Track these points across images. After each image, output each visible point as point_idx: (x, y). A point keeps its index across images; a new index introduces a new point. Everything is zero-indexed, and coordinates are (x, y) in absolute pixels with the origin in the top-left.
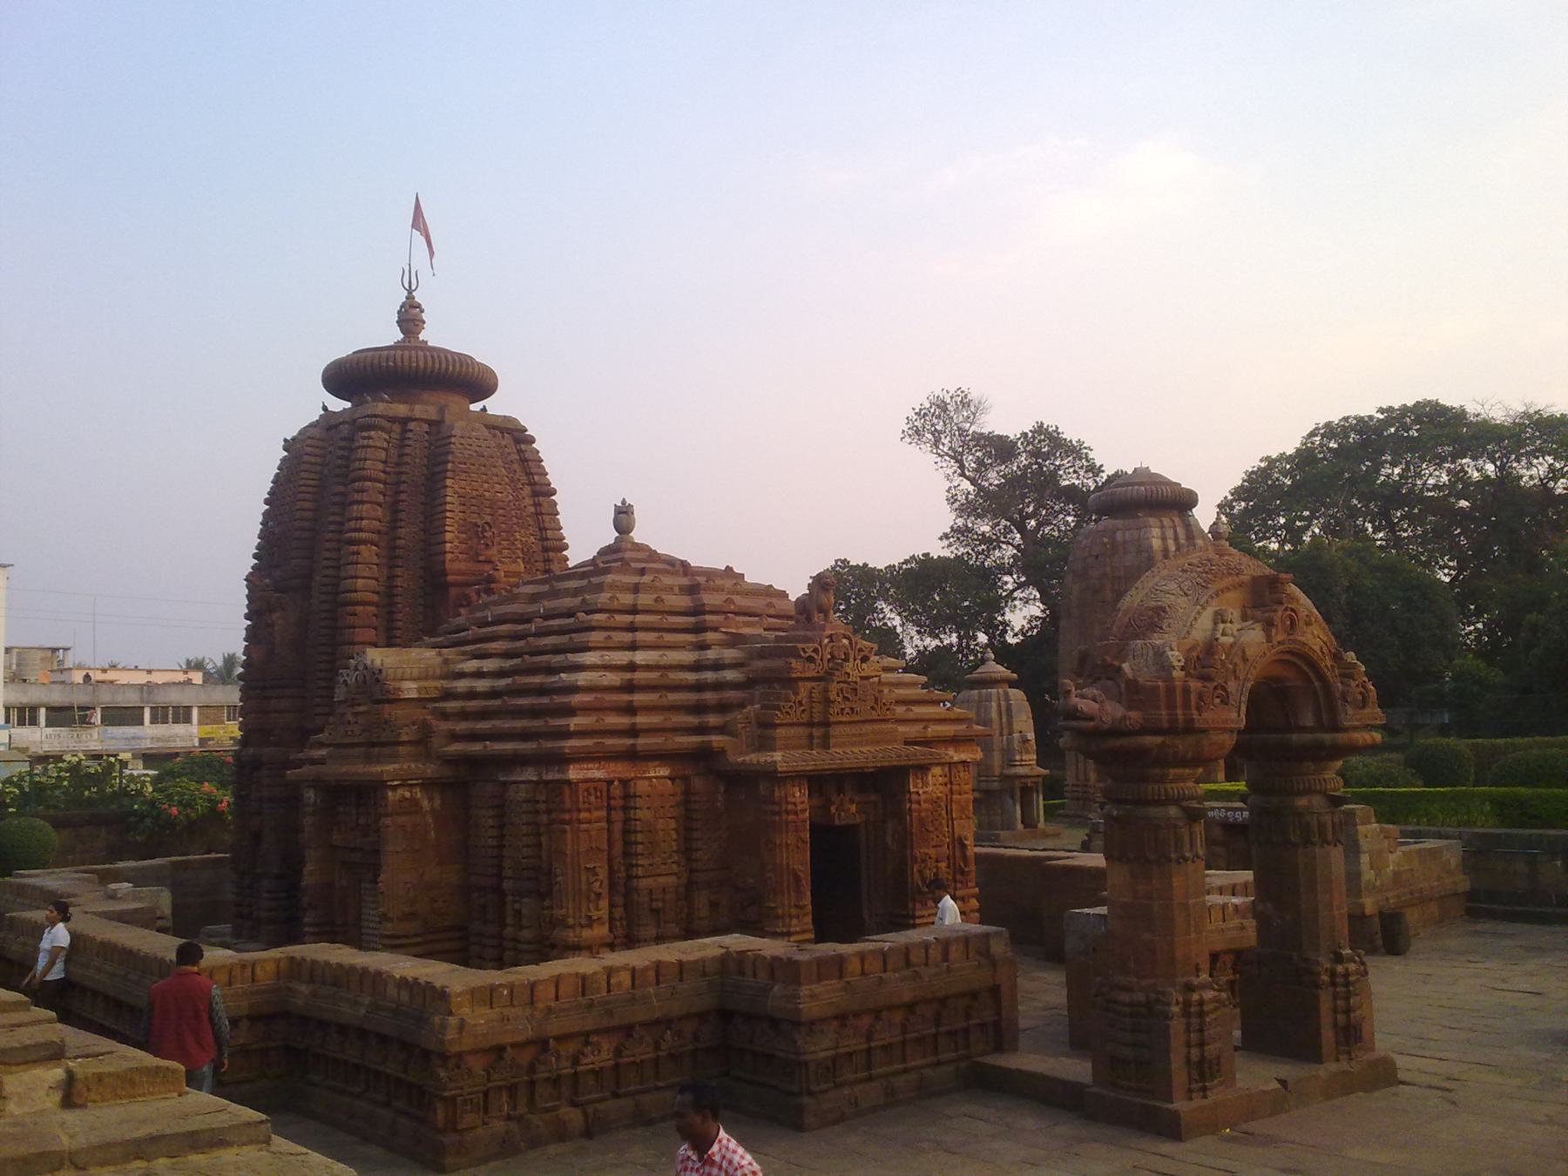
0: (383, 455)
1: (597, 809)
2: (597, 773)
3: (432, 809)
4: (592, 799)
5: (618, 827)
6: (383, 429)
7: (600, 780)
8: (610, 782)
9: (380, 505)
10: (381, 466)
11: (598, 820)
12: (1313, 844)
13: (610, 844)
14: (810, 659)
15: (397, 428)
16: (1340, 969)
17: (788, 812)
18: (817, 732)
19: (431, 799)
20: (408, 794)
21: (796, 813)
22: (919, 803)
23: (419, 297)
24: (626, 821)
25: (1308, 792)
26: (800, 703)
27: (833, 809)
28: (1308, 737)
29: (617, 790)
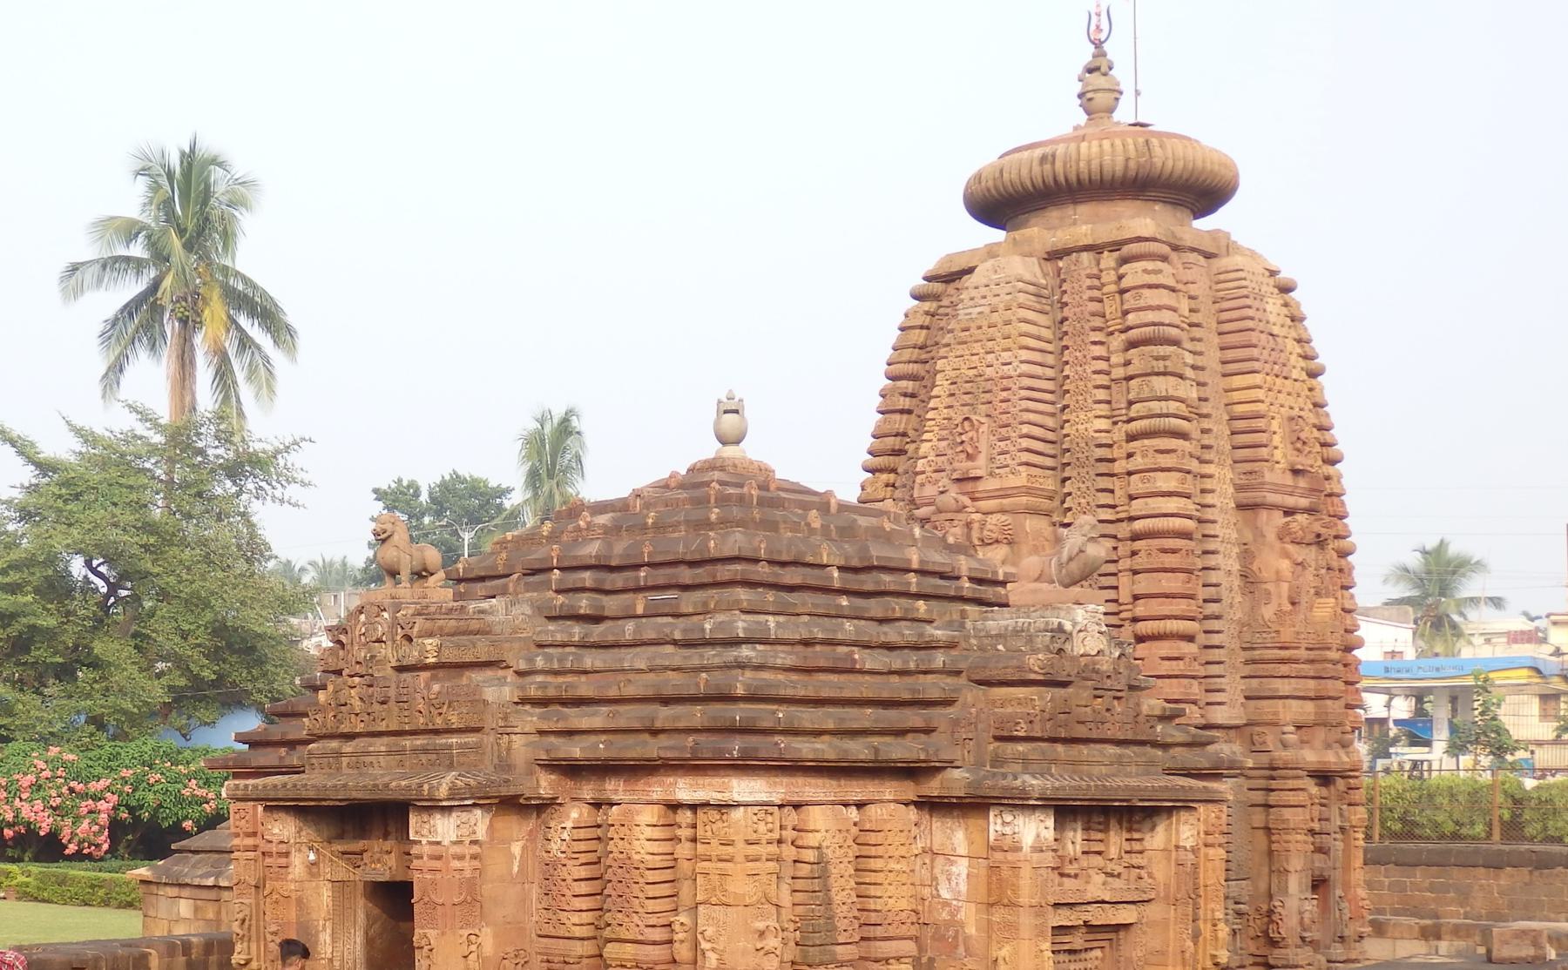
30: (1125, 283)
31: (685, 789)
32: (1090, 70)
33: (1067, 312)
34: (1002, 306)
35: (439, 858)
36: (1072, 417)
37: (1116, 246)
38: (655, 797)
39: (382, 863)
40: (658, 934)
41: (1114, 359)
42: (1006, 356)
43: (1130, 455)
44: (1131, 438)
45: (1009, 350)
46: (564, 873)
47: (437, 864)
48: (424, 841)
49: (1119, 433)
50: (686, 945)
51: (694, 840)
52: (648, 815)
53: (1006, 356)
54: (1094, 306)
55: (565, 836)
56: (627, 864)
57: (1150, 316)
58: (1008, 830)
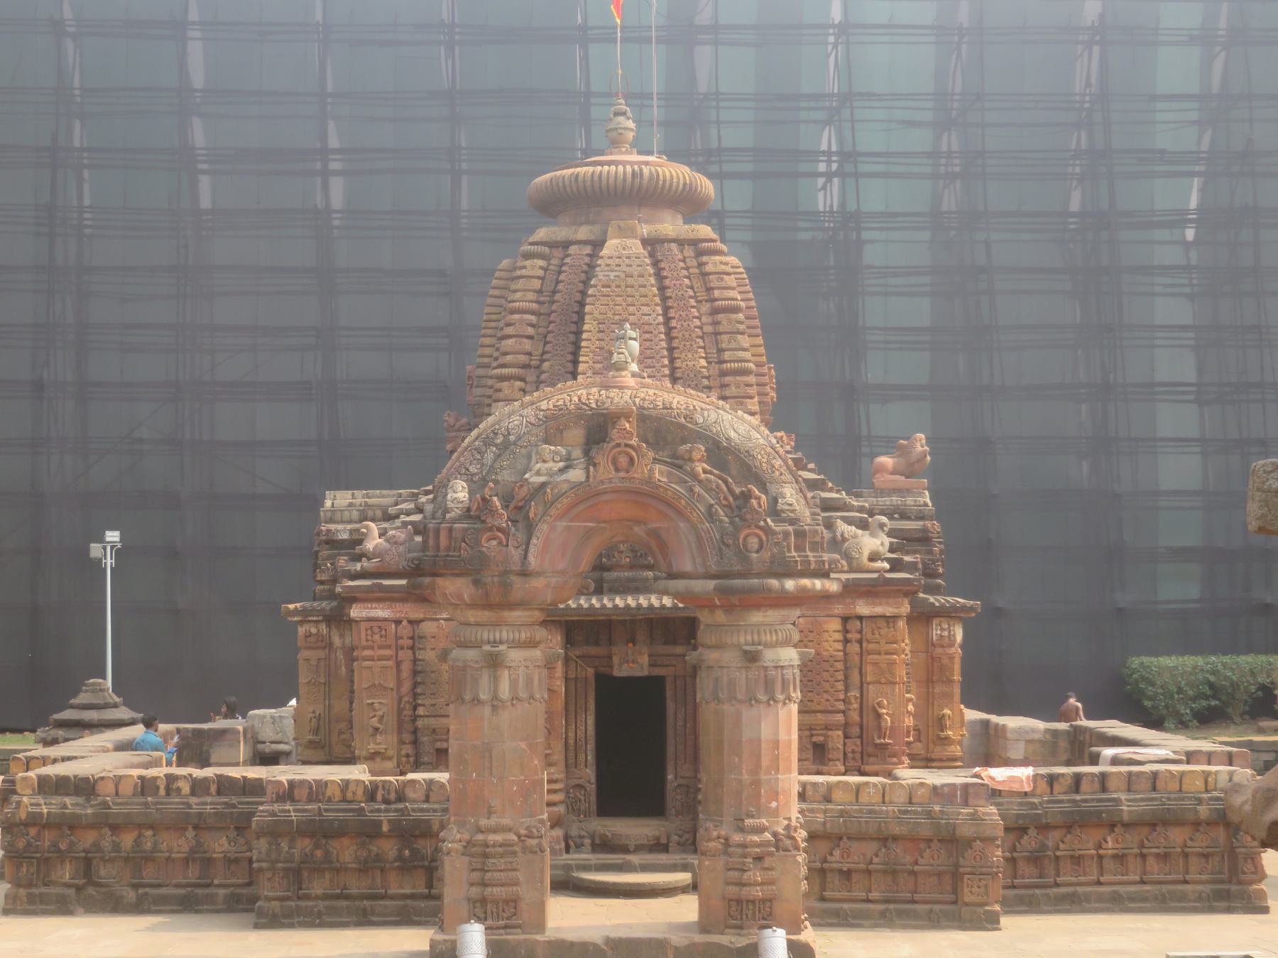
0: (537, 284)
1: (380, 647)
2: (381, 612)
3: (344, 646)
4: (377, 637)
5: (406, 668)
7: (385, 620)
8: (398, 622)
9: (530, 337)
10: (531, 296)
11: (387, 658)
13: (399, 683)
15: (558, 253)
16: (737, 838)
19: (342, 636)
20: (314, 630)
24: (415, 661)
25: (718, 647)
27: (616, 660)
29: (405, 630)
31: (863, 609)
33: (667, 282)
34: (636, 273)
36: (683, 356)
37: (694, 242)
38: (836, 611)
39: (633, 663)
40: (841, 706)
41: (704, 319)
42: (645, 309)
43: (723, 386)
44: (723, 374)
45: (647, 305)
49: (715, 369)
50: (857, 712)
51: (860, 642)
52: (835, 625)
53: (645, 309)
54: (687, 281)
57: (731, 294)
58: (946, 633)
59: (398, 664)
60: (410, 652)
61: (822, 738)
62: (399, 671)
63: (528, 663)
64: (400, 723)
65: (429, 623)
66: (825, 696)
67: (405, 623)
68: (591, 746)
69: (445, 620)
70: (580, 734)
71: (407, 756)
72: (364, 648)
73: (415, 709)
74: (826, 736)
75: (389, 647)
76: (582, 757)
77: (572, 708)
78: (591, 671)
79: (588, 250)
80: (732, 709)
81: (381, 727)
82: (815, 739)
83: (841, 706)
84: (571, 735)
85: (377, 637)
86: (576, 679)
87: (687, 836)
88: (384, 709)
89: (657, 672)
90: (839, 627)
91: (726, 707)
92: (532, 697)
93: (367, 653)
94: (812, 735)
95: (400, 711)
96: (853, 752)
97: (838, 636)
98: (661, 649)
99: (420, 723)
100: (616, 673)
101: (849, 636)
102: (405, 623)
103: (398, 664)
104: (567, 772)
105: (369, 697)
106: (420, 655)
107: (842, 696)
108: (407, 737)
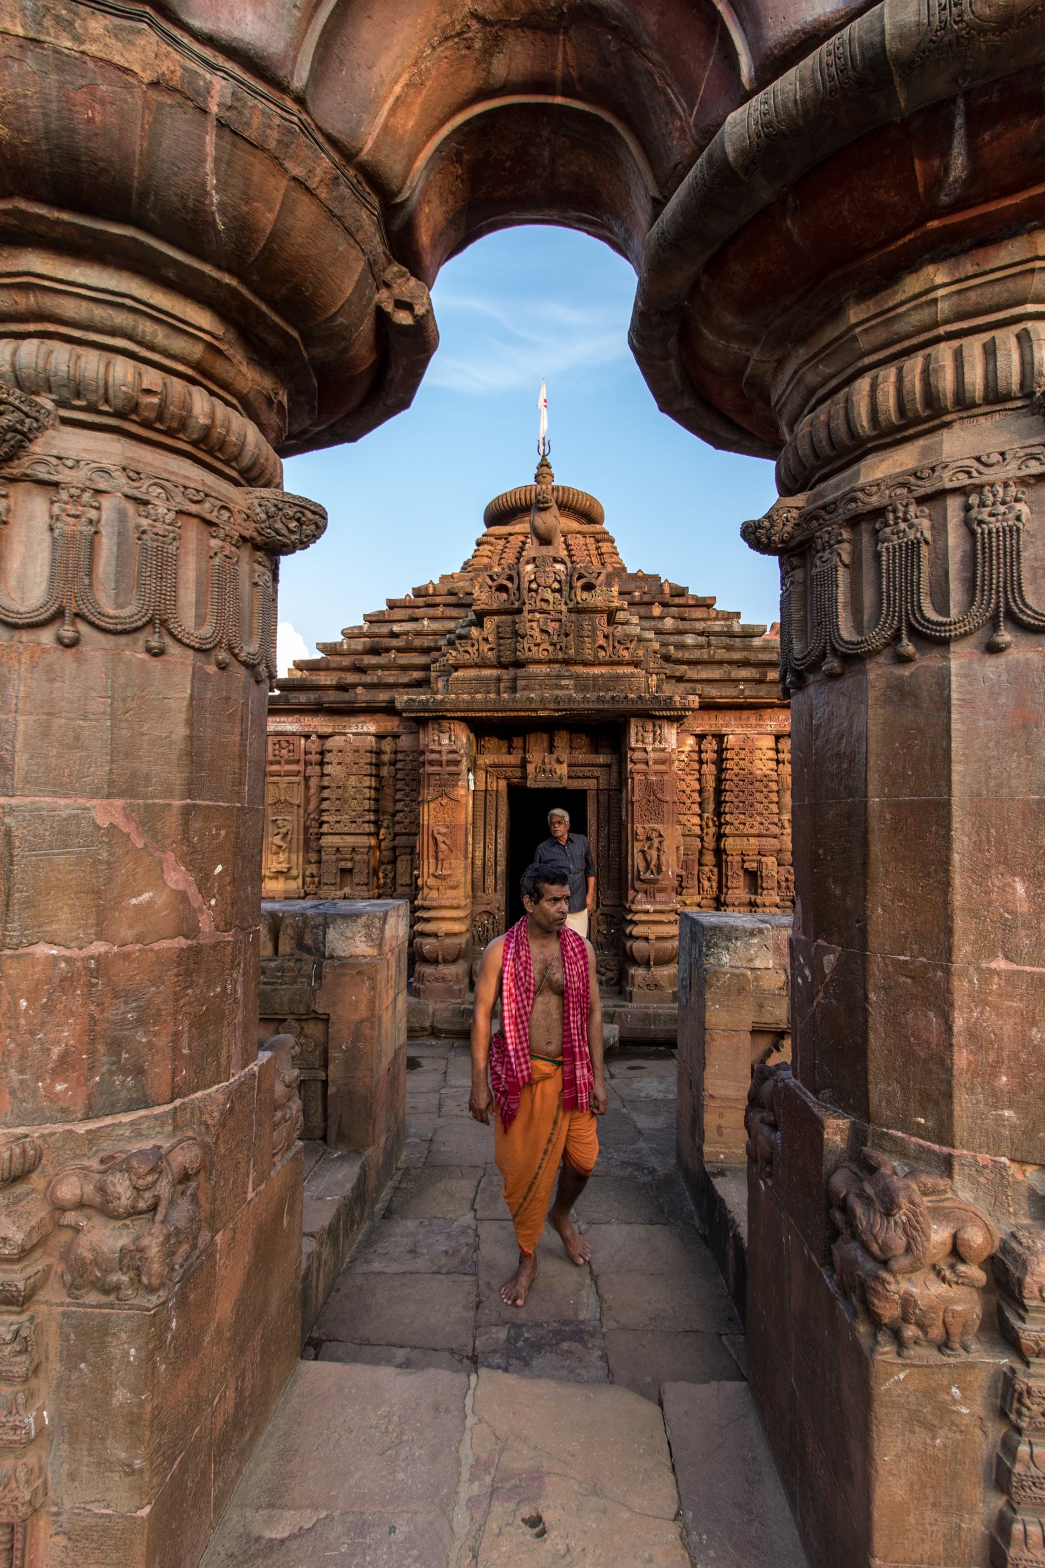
1: (289, 762)
4: (284, 752)
6: (491, 544)
7: (293, 734)
8: (307, 737)
11: (297, 774)
12: (937, 642)
13: (307, 799)
14: (502, 588)
15: (502, 542)
17: (431, 763)
18: (506, 674)
21: (440, 763)
22: (647, 763)
23: (549, 459)
25: (925, 416)
26: (486, 640)
27: (530, 768)
28: (789, 84)
29: (314, 744)
30: (603, 550)
32: (541, 465)
35: (662, 762)
46: (683, 786)
47: (662, 768)
48: (649, 748)
52: (769, 742)
55: (683, 757)
56: (749, 779)
59: (307, 779)
60: (318, 768)
61: (755, 865)
62: (307, 787)
63: (144, 489)
64: (307, 841)
65: (337, 738)
66: (758, 818)
67: (314, 737)
68: (501, 868)
69: (354, 734)
70: (490, 854)
71: (312, 876)
72: (272, 763)
73: (320, 826)
74: (760, 862)
75: (297, 762)
76: (490, 880)
77: (480, 823)
78: (503, 784)
79: (522, 538)
80: (992, 667)
81: (284, 845)
82: (746, 865)
83: (775, 830)
84: (479, 854)
85: (284, 752)
86: (486, 791)
87: (609, 974)
88: (289, 827)
89: (575, 784)
90: (772, 744)
91: (961, 661)
92: (159, 622)
93: (275, 768)
94: (744, 861)
95: (306, 829)
96: (787, 880)
97: (772, 754)
98: (581, 757)
99: (326, 841)
100: (530, 784)
101: (781, 756)
102: (314, 737)
103: (307, 779)
104: (474, 897)
105: (274, 814)
106: (328, 769)
107: (776, 820)
108: (313, 857)
